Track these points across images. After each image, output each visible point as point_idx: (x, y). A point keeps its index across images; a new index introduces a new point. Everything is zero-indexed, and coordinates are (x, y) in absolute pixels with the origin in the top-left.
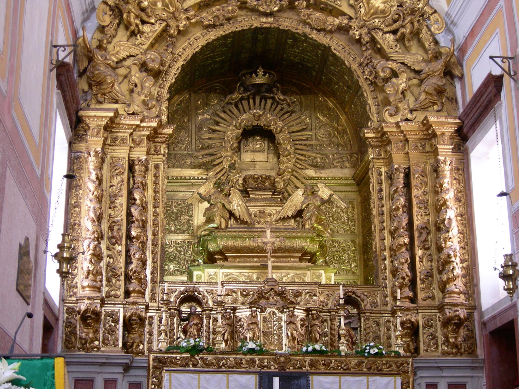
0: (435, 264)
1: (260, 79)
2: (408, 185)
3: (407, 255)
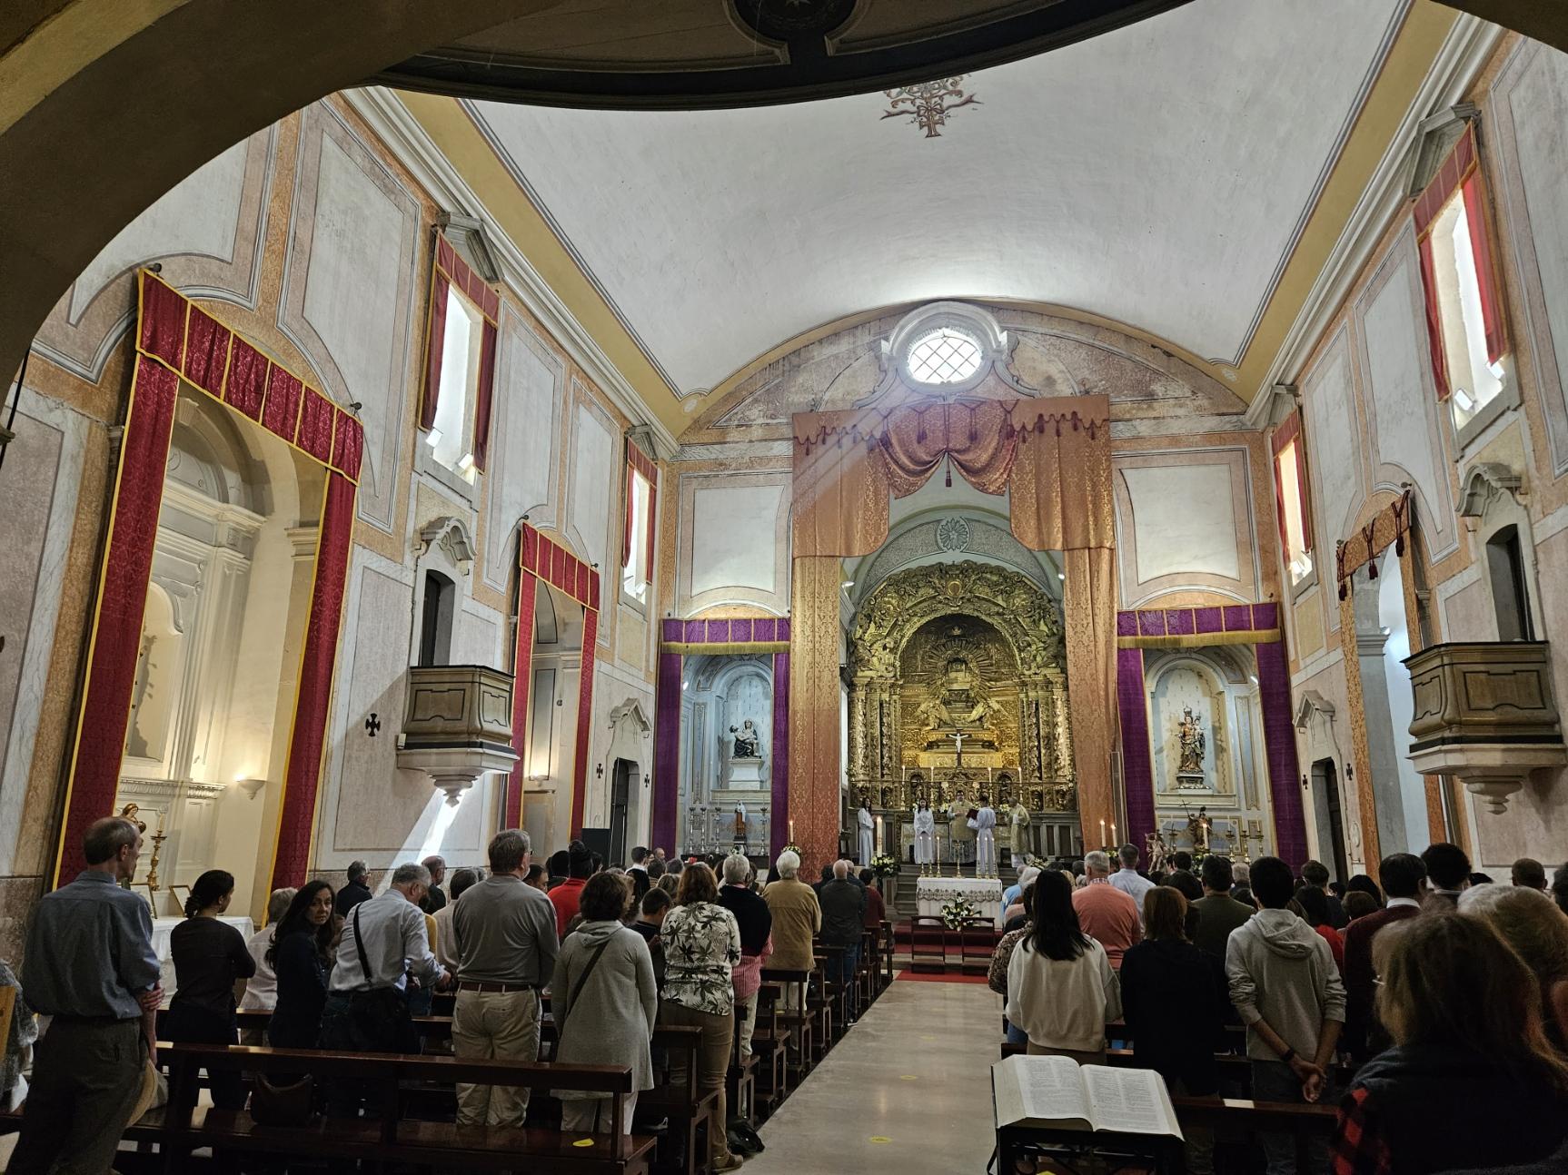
1: (957, 632)
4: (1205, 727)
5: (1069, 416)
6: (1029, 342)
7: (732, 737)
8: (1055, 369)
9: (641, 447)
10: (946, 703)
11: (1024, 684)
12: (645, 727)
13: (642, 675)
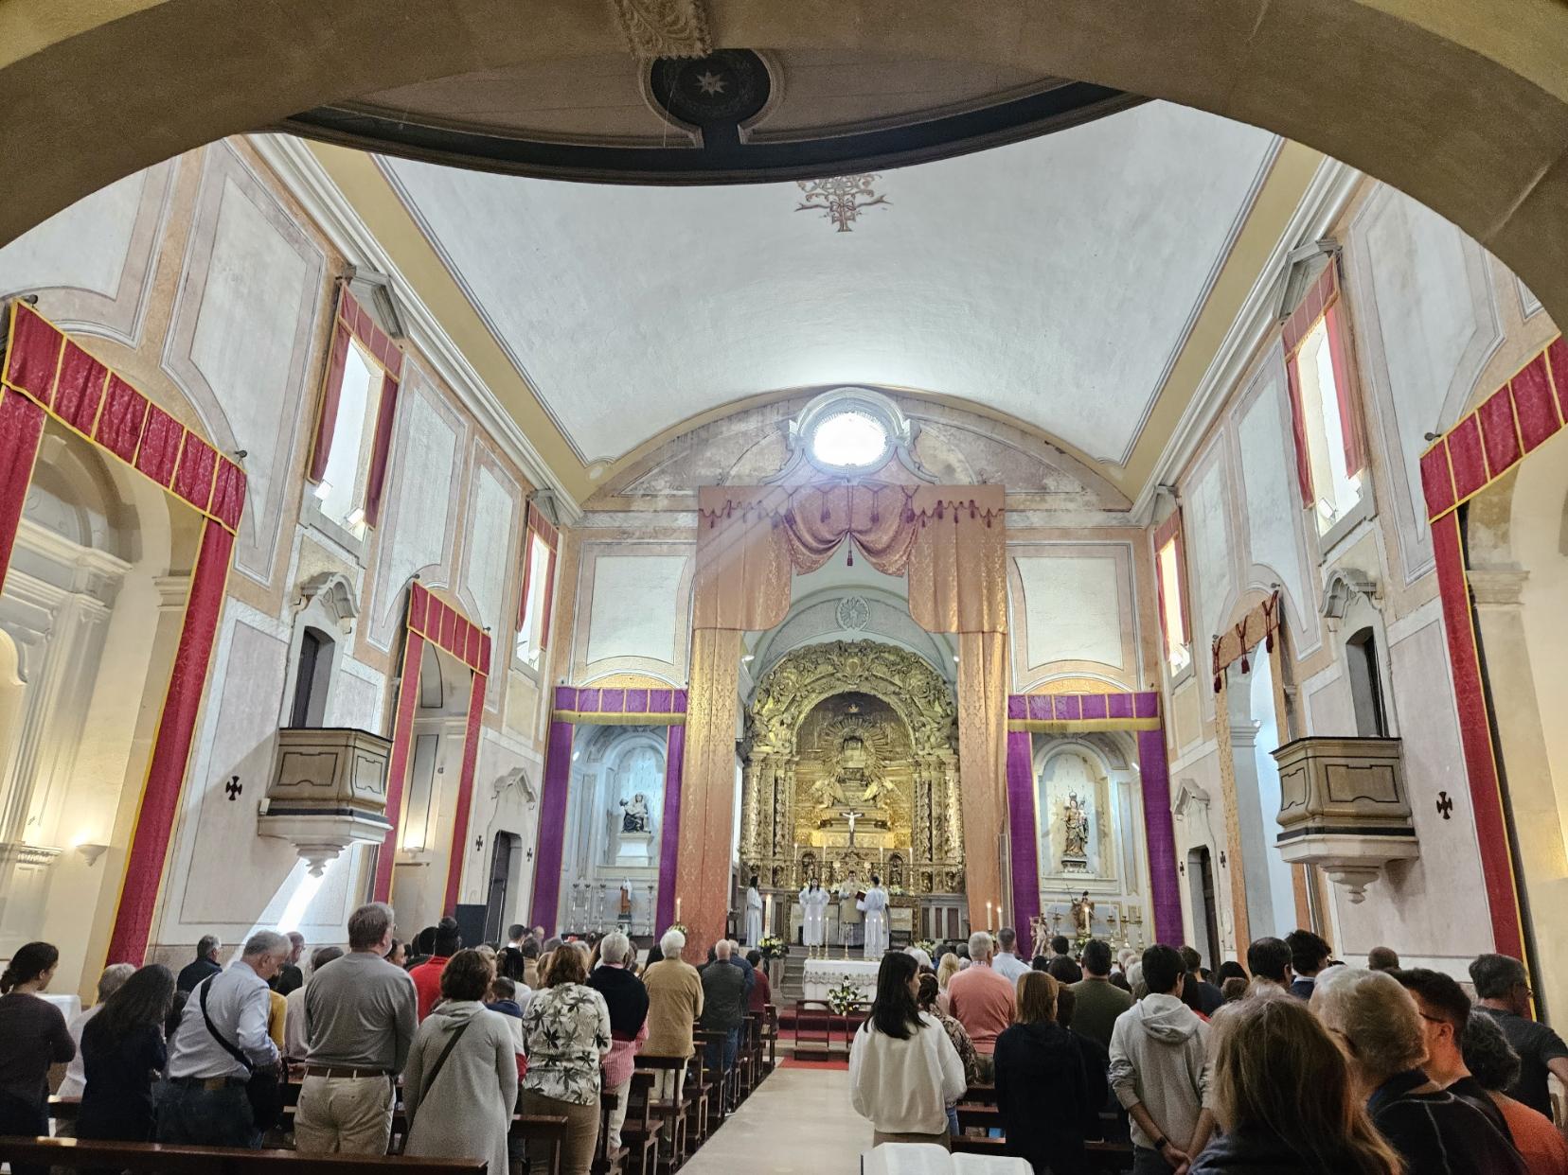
1: (854, 710)
4: (1089, 812)
5: (966, 504)
6: (931, 431)
7: (622, 811)
8: (954, 458)
9: (542, 511)
10: (841, 781)
11: (918, 764)
12: (530, 797)
13: (531, 743)
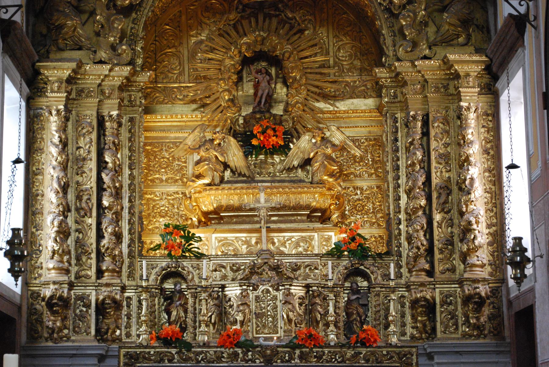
0: (456, 231)
2: (426, 134)
3: (424, 221)
